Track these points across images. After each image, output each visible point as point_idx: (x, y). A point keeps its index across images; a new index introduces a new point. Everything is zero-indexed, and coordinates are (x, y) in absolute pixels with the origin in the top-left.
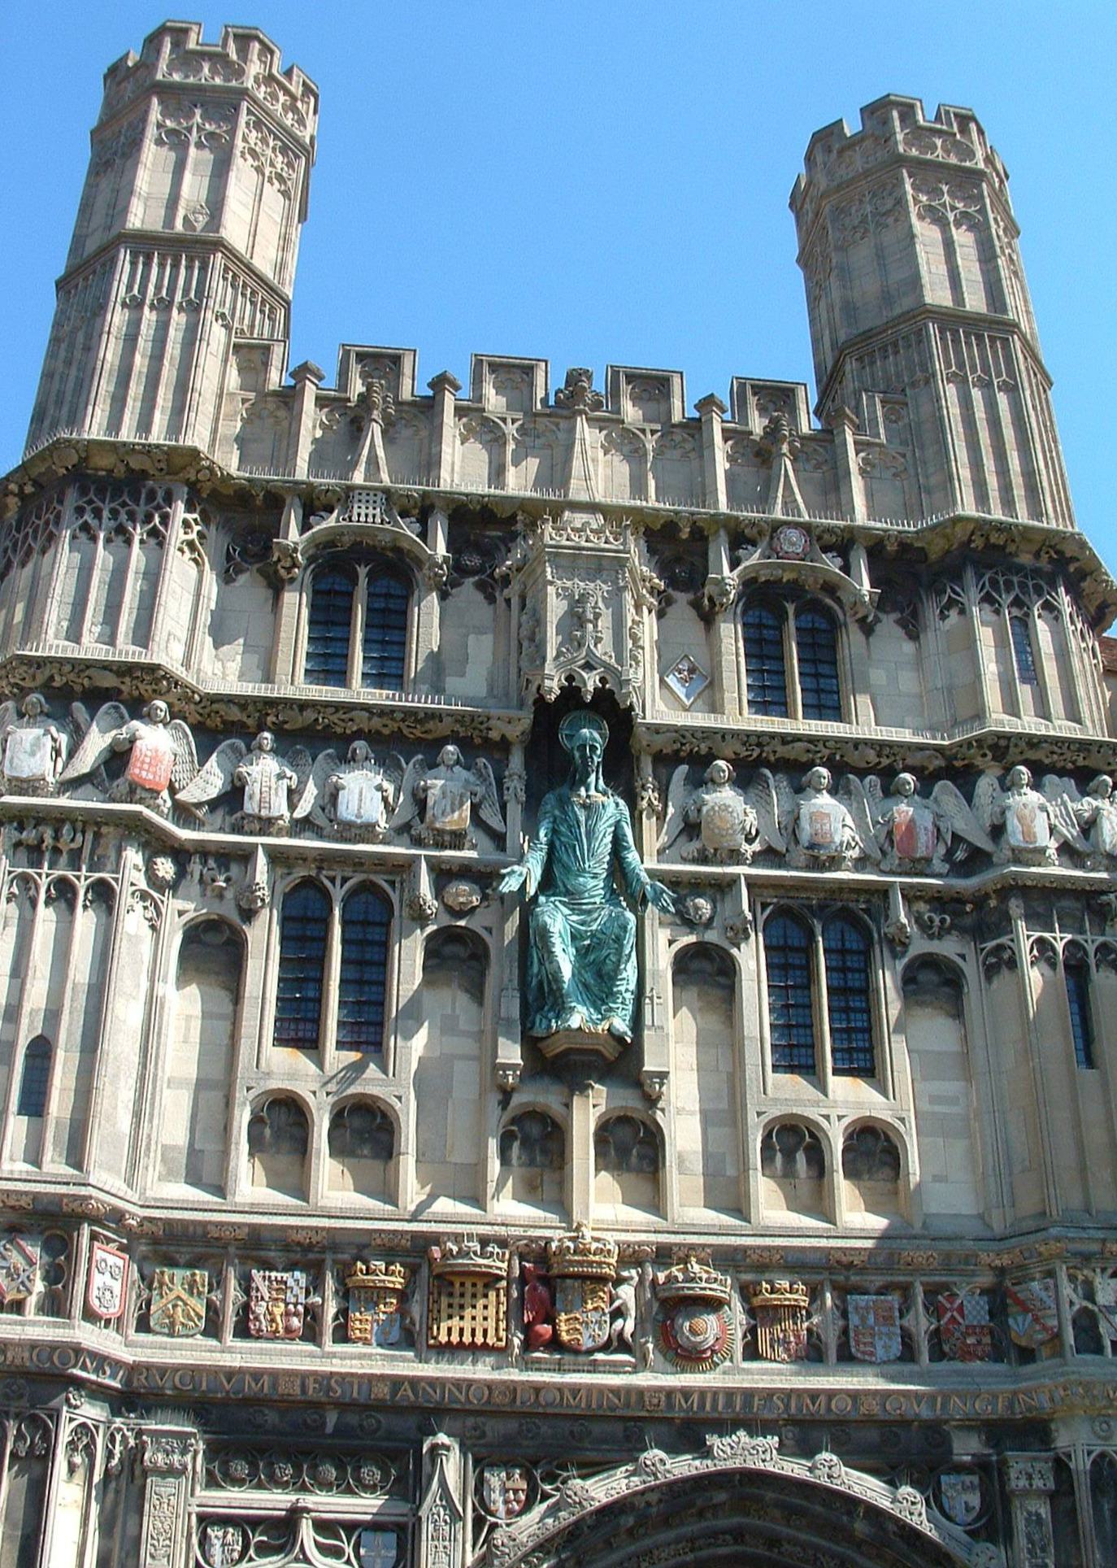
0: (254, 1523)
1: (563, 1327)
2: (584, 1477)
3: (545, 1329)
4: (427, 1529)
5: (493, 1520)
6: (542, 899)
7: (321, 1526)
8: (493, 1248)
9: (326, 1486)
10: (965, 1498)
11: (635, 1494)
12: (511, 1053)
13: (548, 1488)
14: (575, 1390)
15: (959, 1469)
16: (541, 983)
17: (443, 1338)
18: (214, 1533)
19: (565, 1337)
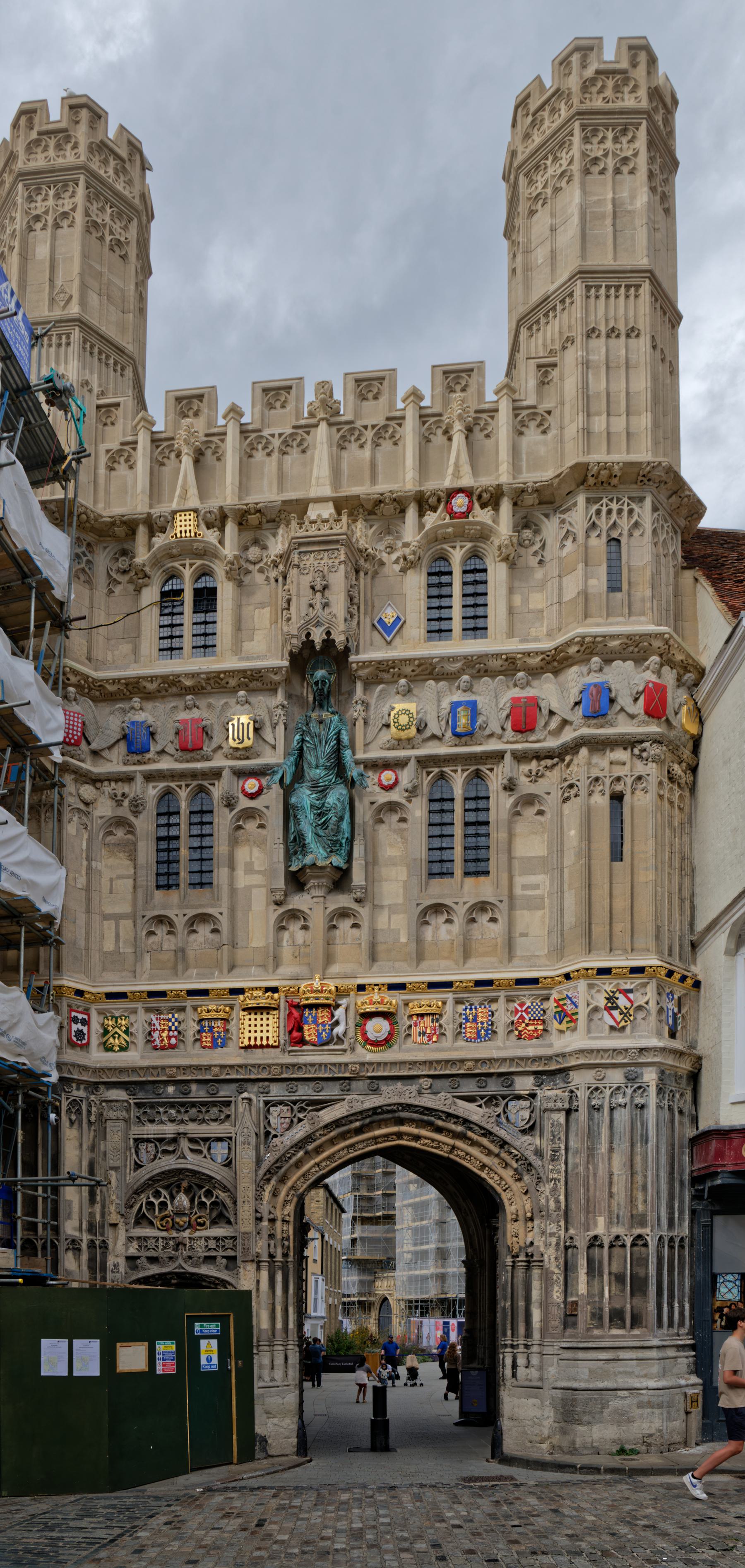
0: (161, 1140)
1: (306, 1033)
2: (318, 1110)
3: (295, 1034)
4: (240, 1139)
5: (273, 1132)
6: (296, 785)
7: (191, 1140)
8: (269, 994)
9: (193, 1120)
10: (520, 1112)
11: (343, 1118)
12: (280, 883)
13: (301, 1116)
14: (312, 1065)
15: (519, 1097)
16: (295, 838)
17: (246, 1043)
18: (142, 1147)
19: (307, 1038)
